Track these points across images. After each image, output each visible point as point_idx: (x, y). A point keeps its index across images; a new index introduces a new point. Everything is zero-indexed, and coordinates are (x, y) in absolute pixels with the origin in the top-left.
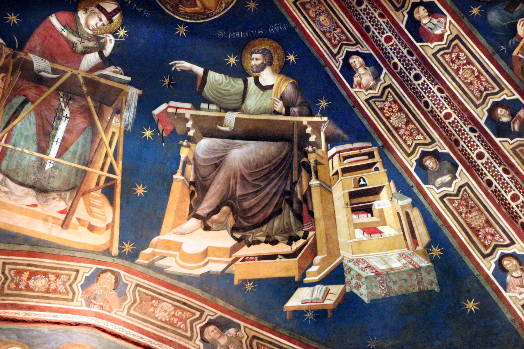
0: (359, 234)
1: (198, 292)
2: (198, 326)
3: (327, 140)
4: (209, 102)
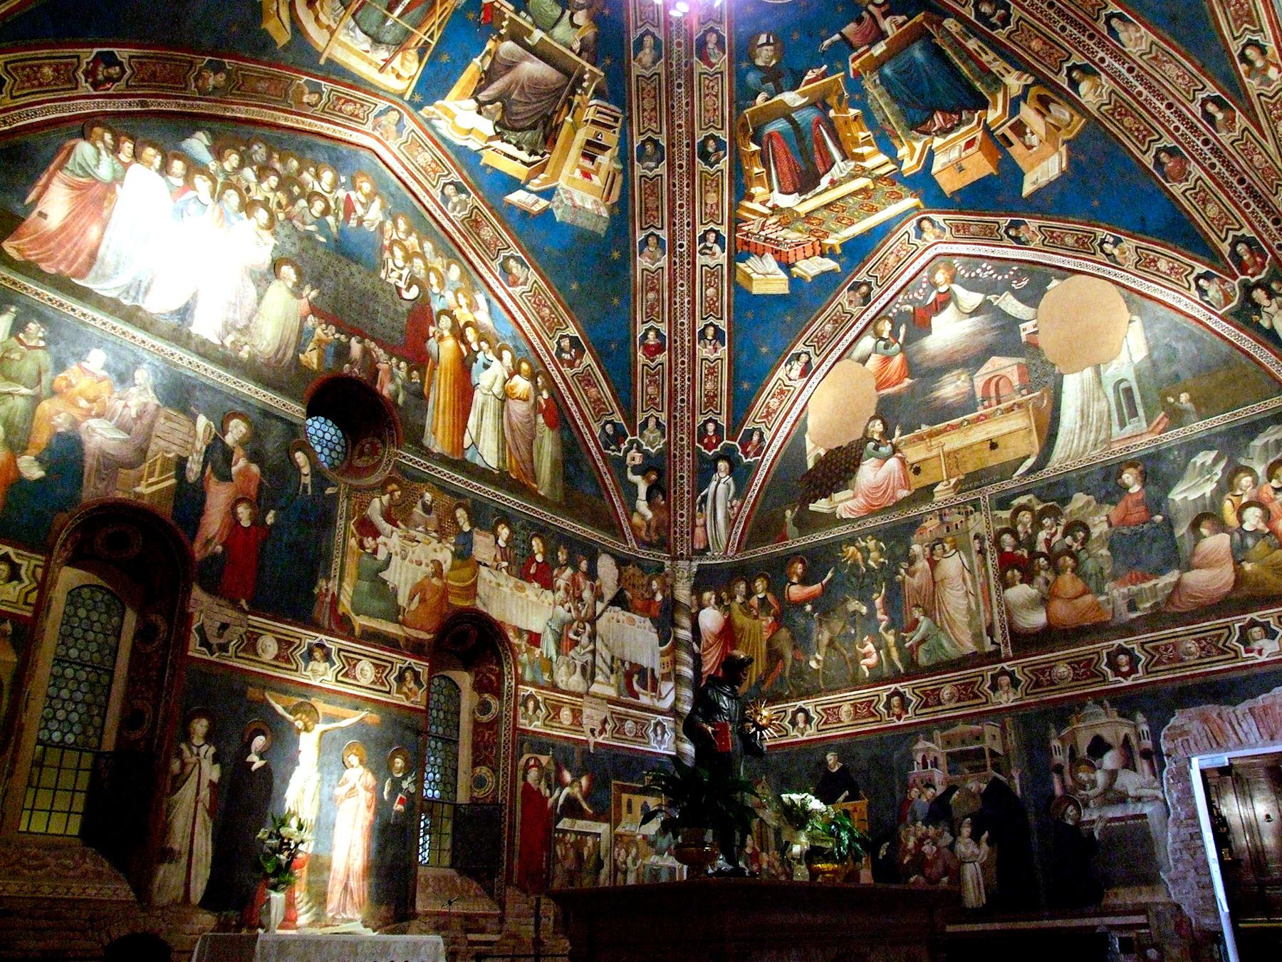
0: (578, 173)
1: (453, 157)
2: (443, 181)
3: (594, 92)
4: (528, 13)
